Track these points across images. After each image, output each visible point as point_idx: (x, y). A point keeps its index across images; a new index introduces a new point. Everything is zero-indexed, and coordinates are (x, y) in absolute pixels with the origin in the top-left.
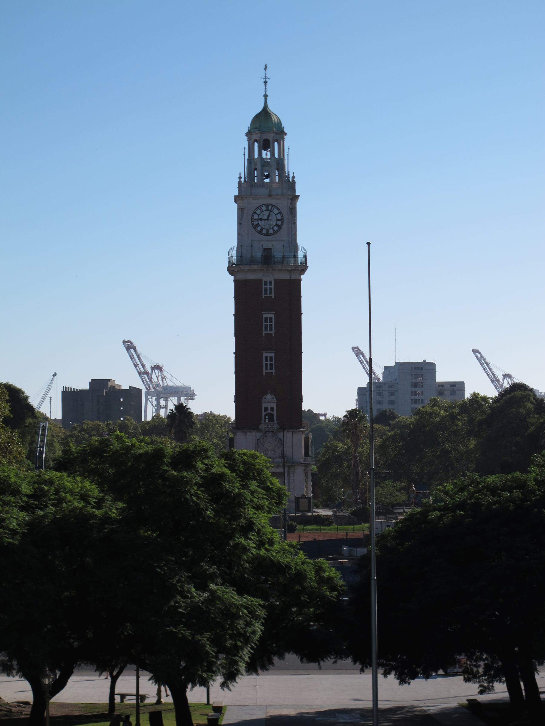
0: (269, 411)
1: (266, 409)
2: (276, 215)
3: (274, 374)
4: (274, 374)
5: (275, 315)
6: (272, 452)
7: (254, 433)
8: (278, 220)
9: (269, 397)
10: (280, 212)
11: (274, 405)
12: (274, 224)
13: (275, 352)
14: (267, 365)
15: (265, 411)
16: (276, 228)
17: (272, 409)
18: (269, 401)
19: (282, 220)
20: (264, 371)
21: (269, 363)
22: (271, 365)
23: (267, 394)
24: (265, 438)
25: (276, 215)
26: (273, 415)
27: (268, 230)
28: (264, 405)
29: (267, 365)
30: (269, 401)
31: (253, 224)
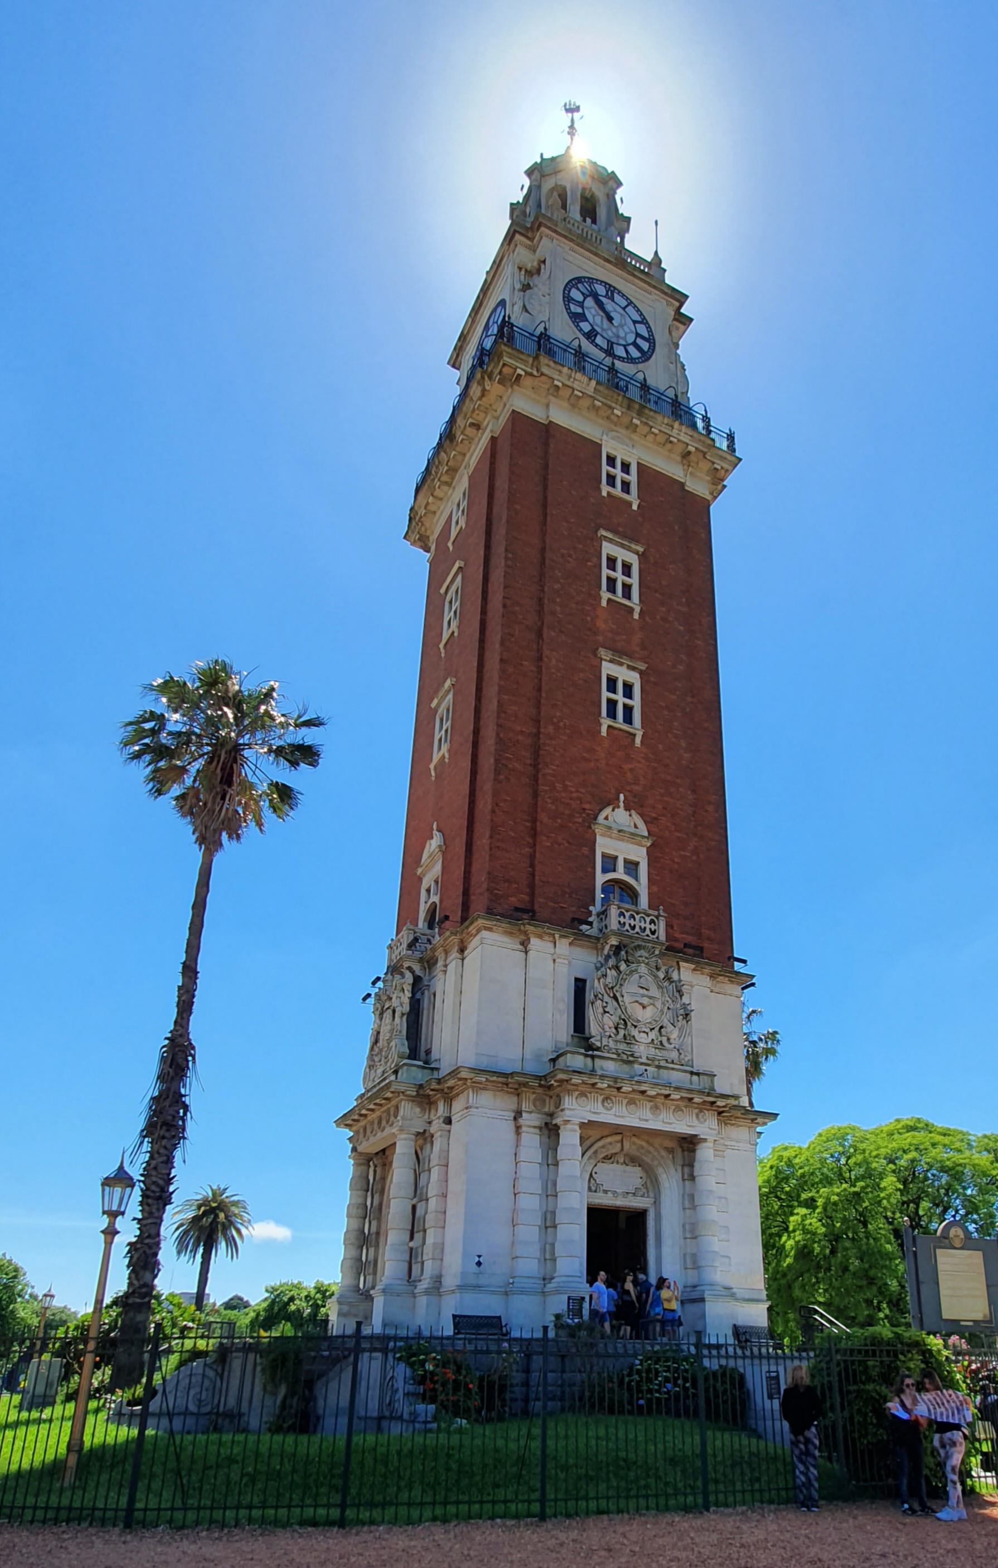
0: (620, 874)
1: (610, 863)
2: (635, 322)
3: (638, 741)
4: (638, 741)
5: (642, 557)
6: (653, 1035)
7: (563, 946)
8: (638, 335)
9: (620, 817)
10: (644, 321)
11: (639, 854)
12: (631, 338)
13: (643, 667)
14: (612, 704)
15: (605, 871)
16: (635, 353)
17: (632, 866)
18: (621, 839)
19: (651, 340)
20: (606, 722)
21: (620, 697)
22: (628, 710)
23: (613, 803)
24: (623, 966)
25: (635, 322)
26: (633, 895)
27: (610, 343)
28: (603, 845)
29: (612, 704)
30: (621, 839)
31: (568, 309)
